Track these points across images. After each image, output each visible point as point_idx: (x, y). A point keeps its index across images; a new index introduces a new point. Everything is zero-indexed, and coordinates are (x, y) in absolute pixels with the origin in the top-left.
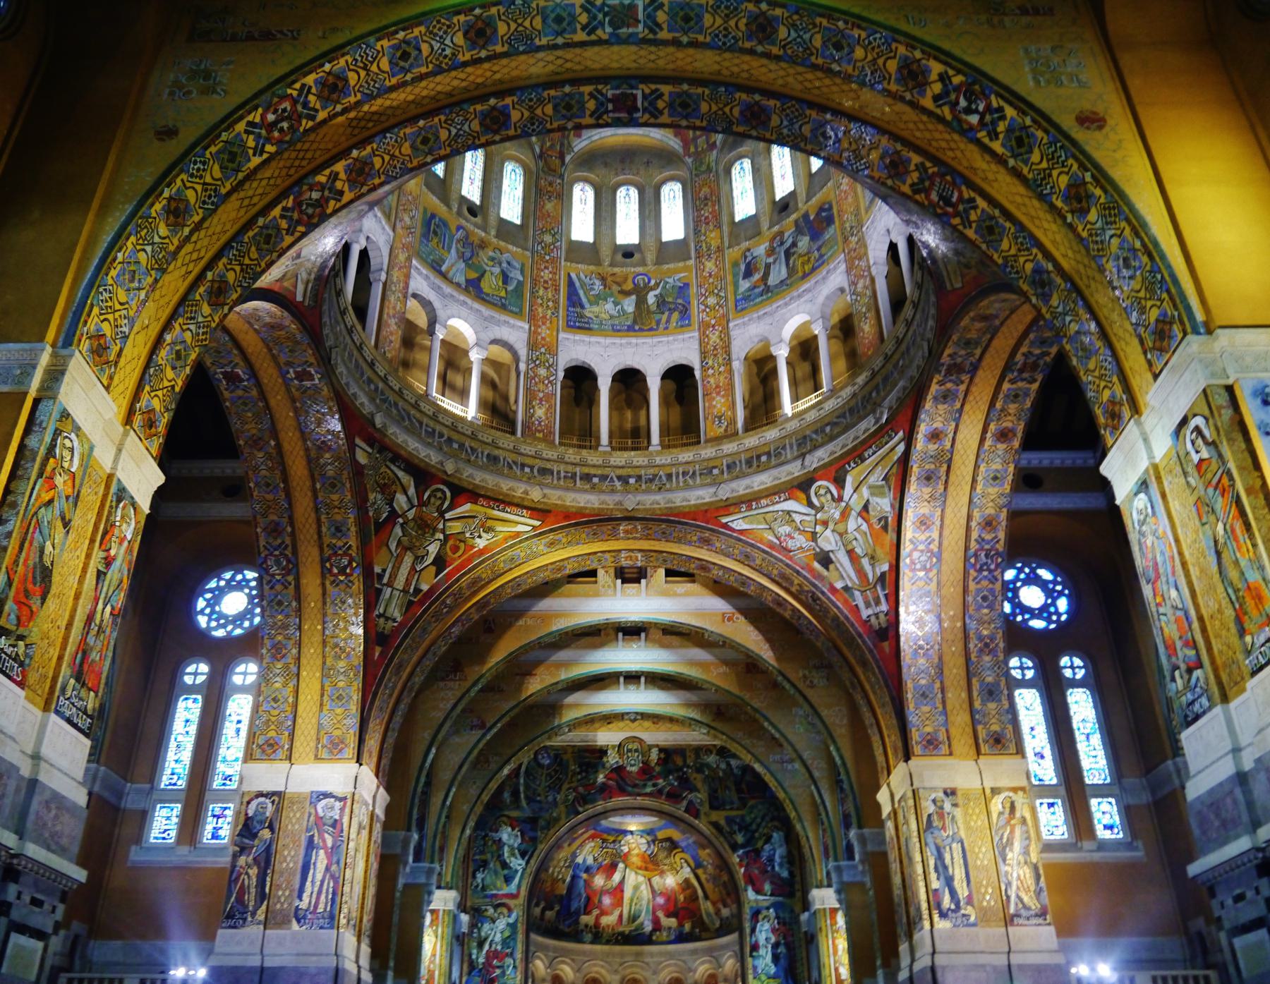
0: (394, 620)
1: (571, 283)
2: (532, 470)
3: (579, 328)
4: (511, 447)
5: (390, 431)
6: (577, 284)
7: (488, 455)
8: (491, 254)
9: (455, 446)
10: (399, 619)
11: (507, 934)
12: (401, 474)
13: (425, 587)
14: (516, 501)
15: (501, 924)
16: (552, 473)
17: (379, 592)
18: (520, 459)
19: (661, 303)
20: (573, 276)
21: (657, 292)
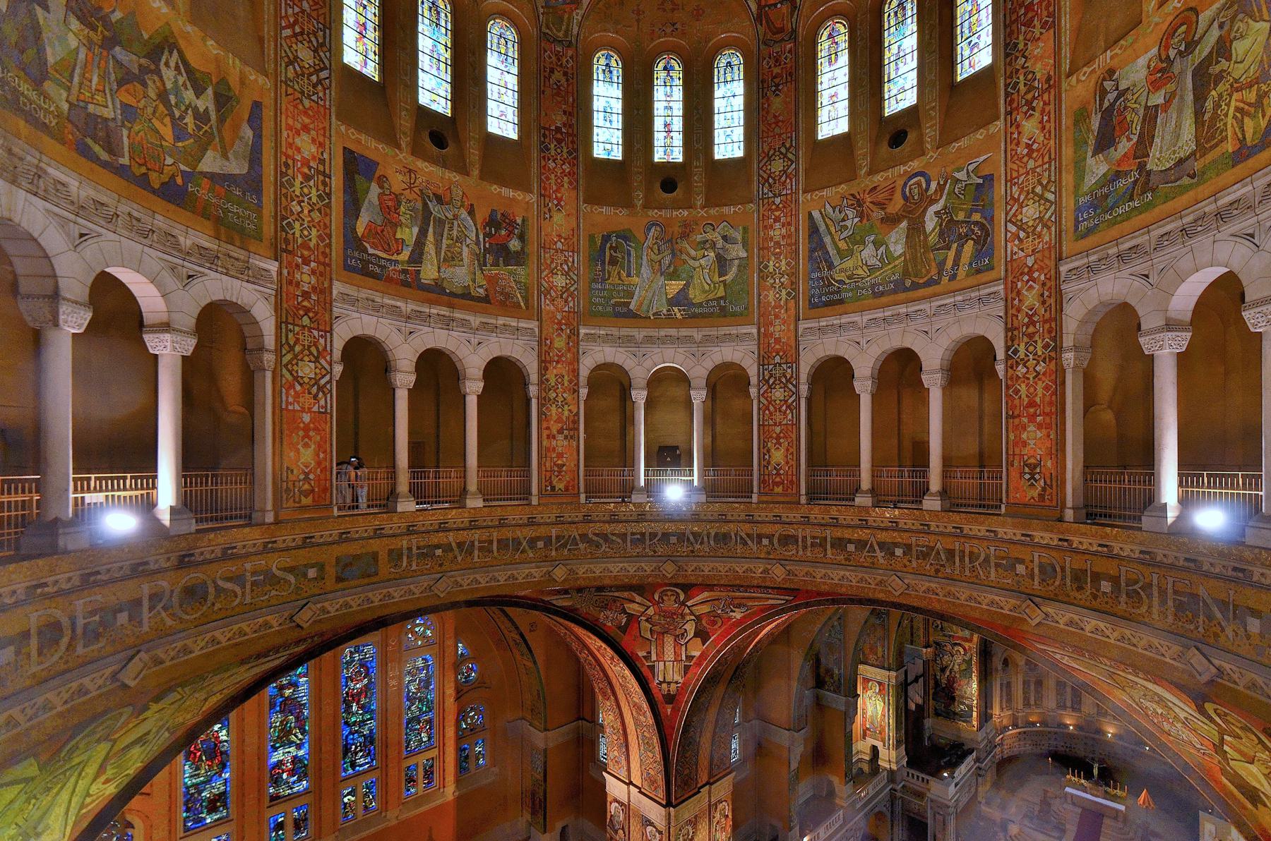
0: (677, 683)
1: (814, 230)
2: (771, 543)
3: (827, 304)
4: (743, 517)
5: (581, 572)
6: (822, 228)
7: (716, 534)
8: (699, 238)
9: (673, 540)
10: (681, 681)
11: (964, 667)
12: (616, 594)
13: (697, 654)
14: (755, 582)
15: (958, 660)
16: (797, 541)
17: (652, 668)
18: (756, 530)
19: (948, 225)
20: (816, 214)
21: (938, 207)
